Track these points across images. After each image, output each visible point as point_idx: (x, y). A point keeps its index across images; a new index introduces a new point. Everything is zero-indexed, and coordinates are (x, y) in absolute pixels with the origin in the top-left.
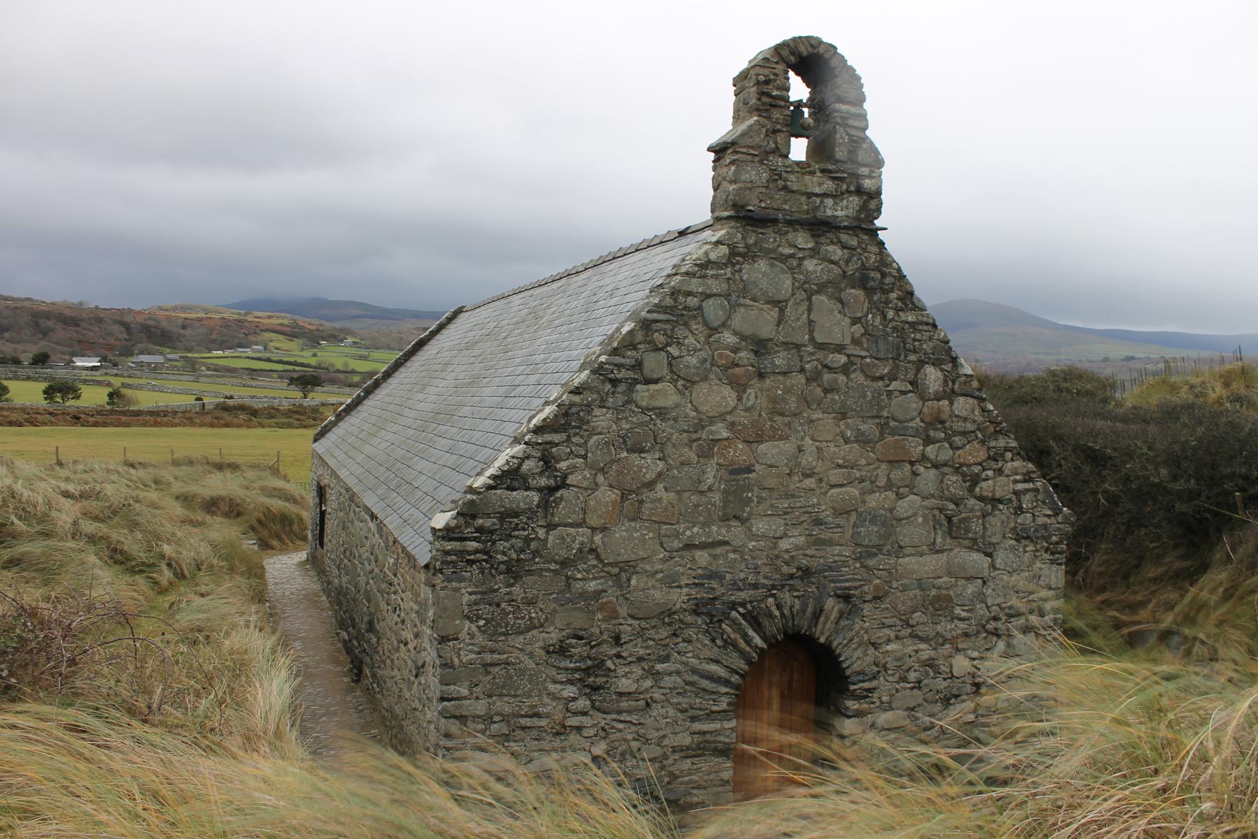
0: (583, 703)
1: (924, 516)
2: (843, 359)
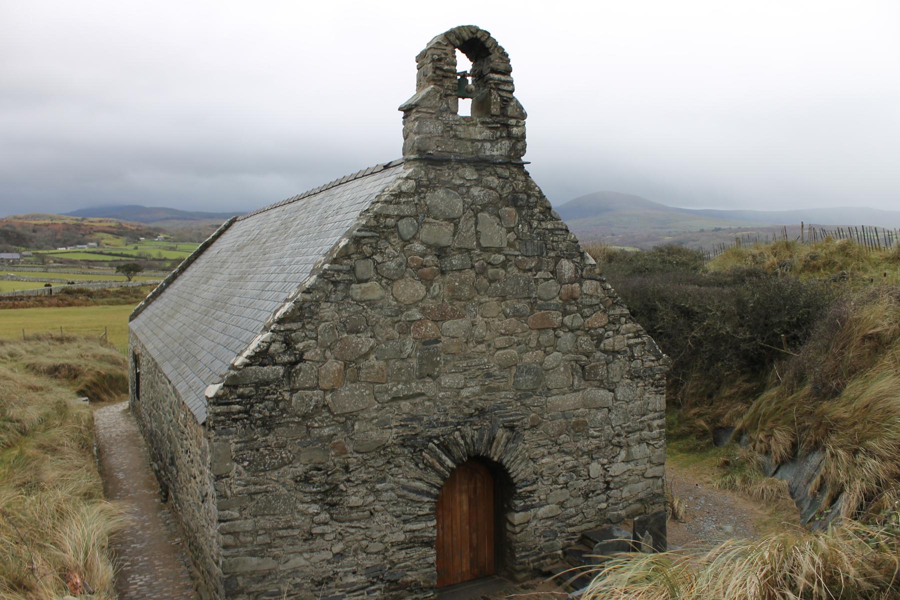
0: (324, 516)
1: (565, 367)
2: (502, 258)
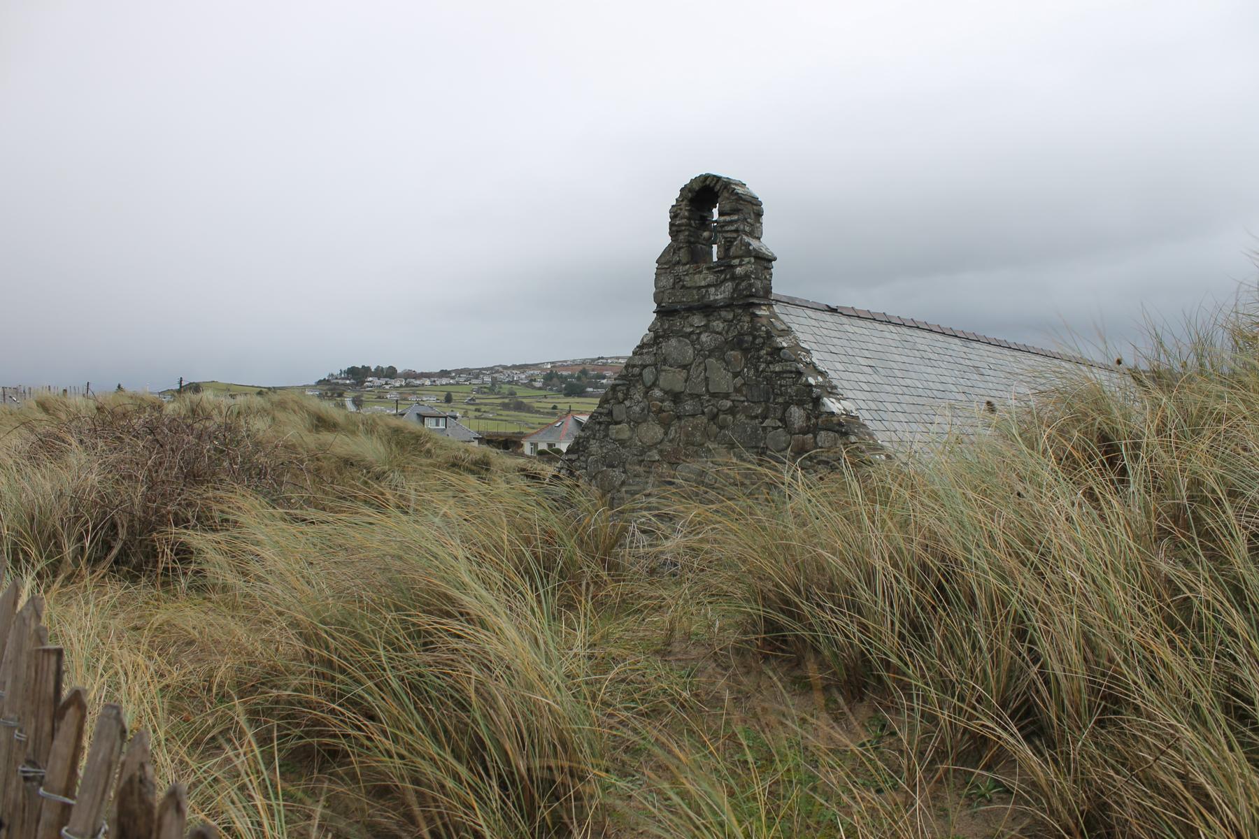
2: (729, 404)
